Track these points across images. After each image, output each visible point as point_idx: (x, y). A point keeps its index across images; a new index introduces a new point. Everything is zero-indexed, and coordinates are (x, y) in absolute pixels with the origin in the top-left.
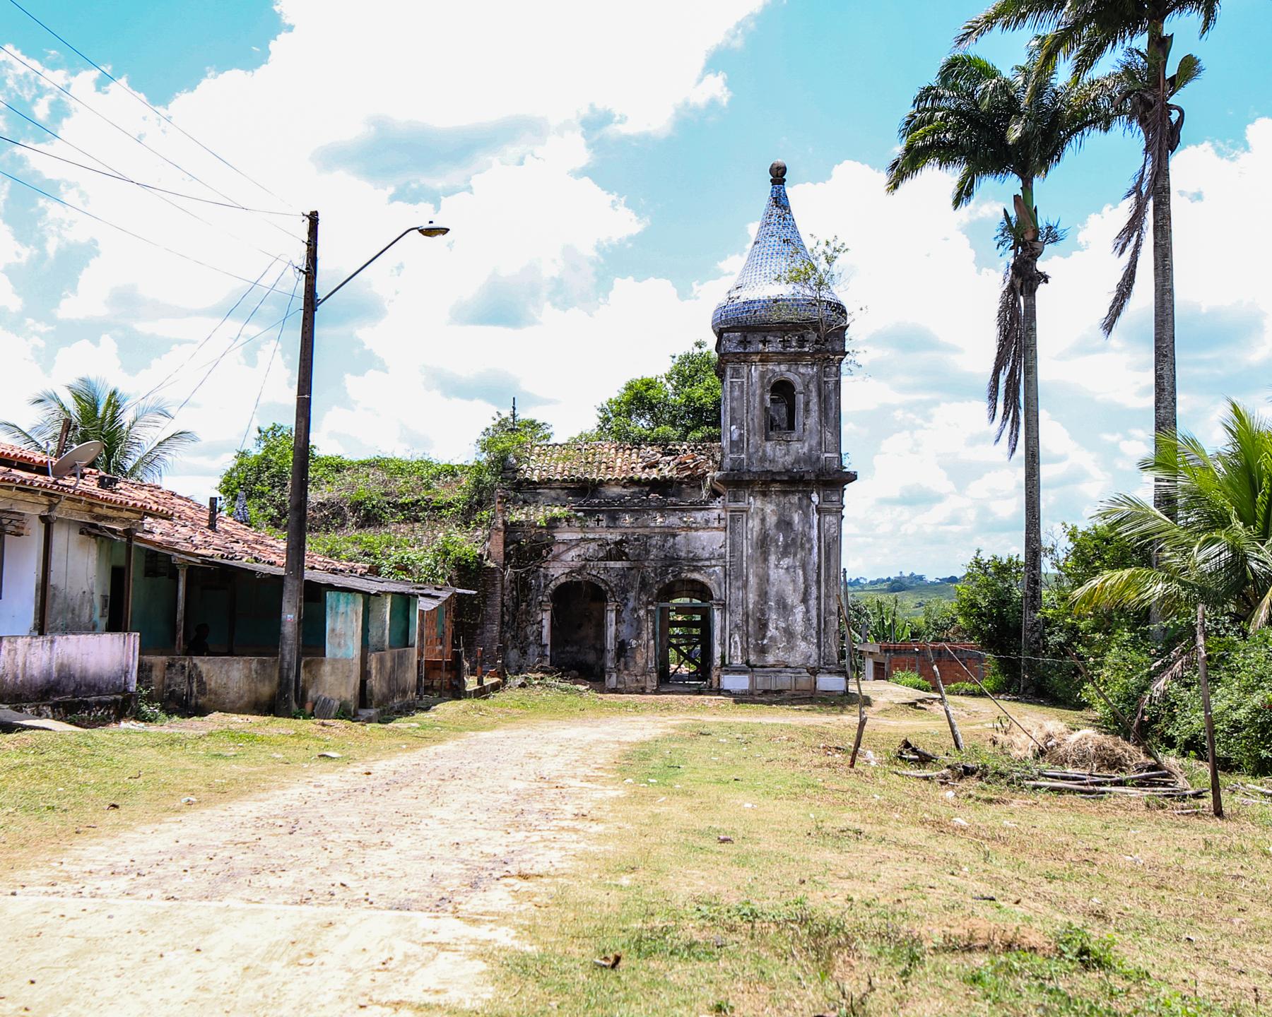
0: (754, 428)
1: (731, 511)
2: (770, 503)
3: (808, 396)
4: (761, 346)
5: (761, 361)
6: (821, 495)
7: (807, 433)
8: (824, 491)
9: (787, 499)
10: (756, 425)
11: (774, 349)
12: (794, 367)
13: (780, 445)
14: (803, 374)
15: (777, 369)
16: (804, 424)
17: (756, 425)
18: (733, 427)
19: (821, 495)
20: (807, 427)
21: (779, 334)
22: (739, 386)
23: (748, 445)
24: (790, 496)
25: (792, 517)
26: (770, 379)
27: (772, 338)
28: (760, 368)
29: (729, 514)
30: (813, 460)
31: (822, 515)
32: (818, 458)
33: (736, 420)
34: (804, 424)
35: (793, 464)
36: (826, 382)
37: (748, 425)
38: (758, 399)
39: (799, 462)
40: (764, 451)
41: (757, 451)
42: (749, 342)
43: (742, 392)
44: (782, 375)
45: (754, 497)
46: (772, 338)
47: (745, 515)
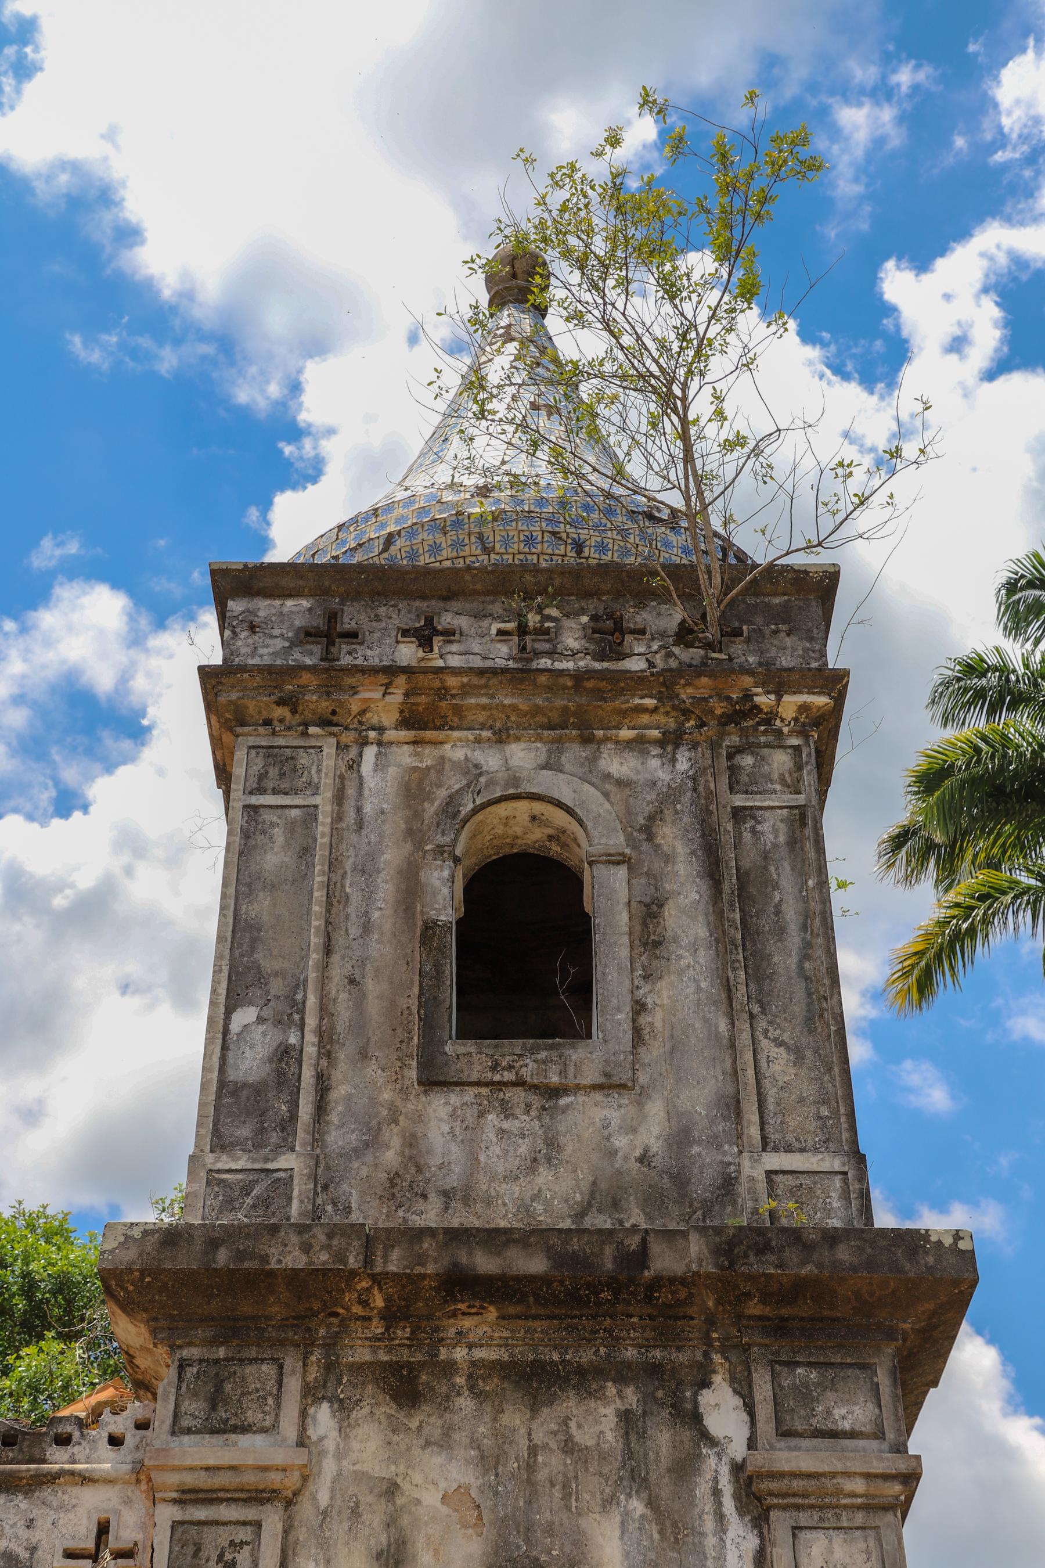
0: (359, 1025)
1: (188, 1497)
2: (444, 1443)
3: (654, 879)
4: (408, 653)
5: (410, 720)
6: (763, 1390)
7: (655, 1050)
8: (777, 1364)
9: (546, 1423)
10: (374, 1008)
11: (477, 662)
12: (574, 753)
13: (506, 1110)
15: (491, 760)
16: (639, 1008)
17: (374, 1008)
18: (244, 1017)
19: (763, 1390)
20: (656, 1019)
21: (497, 608)
22: (291, 827)
23: (321, 1109)
24: (569, 1404)
25: (579, 1541)
26: (452, 801)
27: (462, 622)
28: (404, 756)
29: (167, 1513)
30: (702, 1185)
31: (780, 1523)
32: (728, 1184)
33: (261, 978)
34: (639, 1008)
35: (581, 1215)
36: (739, 814)
37: (324, 1010)
38: (386, 890)
39: (616, 1204)
40: (411, 1141)
41: (372, 1142)
42: (352, 635)
43: (306, 851)
44: (515, 781)
45: (343, 1408)
46: (462, 622)
47: (272, 1520)
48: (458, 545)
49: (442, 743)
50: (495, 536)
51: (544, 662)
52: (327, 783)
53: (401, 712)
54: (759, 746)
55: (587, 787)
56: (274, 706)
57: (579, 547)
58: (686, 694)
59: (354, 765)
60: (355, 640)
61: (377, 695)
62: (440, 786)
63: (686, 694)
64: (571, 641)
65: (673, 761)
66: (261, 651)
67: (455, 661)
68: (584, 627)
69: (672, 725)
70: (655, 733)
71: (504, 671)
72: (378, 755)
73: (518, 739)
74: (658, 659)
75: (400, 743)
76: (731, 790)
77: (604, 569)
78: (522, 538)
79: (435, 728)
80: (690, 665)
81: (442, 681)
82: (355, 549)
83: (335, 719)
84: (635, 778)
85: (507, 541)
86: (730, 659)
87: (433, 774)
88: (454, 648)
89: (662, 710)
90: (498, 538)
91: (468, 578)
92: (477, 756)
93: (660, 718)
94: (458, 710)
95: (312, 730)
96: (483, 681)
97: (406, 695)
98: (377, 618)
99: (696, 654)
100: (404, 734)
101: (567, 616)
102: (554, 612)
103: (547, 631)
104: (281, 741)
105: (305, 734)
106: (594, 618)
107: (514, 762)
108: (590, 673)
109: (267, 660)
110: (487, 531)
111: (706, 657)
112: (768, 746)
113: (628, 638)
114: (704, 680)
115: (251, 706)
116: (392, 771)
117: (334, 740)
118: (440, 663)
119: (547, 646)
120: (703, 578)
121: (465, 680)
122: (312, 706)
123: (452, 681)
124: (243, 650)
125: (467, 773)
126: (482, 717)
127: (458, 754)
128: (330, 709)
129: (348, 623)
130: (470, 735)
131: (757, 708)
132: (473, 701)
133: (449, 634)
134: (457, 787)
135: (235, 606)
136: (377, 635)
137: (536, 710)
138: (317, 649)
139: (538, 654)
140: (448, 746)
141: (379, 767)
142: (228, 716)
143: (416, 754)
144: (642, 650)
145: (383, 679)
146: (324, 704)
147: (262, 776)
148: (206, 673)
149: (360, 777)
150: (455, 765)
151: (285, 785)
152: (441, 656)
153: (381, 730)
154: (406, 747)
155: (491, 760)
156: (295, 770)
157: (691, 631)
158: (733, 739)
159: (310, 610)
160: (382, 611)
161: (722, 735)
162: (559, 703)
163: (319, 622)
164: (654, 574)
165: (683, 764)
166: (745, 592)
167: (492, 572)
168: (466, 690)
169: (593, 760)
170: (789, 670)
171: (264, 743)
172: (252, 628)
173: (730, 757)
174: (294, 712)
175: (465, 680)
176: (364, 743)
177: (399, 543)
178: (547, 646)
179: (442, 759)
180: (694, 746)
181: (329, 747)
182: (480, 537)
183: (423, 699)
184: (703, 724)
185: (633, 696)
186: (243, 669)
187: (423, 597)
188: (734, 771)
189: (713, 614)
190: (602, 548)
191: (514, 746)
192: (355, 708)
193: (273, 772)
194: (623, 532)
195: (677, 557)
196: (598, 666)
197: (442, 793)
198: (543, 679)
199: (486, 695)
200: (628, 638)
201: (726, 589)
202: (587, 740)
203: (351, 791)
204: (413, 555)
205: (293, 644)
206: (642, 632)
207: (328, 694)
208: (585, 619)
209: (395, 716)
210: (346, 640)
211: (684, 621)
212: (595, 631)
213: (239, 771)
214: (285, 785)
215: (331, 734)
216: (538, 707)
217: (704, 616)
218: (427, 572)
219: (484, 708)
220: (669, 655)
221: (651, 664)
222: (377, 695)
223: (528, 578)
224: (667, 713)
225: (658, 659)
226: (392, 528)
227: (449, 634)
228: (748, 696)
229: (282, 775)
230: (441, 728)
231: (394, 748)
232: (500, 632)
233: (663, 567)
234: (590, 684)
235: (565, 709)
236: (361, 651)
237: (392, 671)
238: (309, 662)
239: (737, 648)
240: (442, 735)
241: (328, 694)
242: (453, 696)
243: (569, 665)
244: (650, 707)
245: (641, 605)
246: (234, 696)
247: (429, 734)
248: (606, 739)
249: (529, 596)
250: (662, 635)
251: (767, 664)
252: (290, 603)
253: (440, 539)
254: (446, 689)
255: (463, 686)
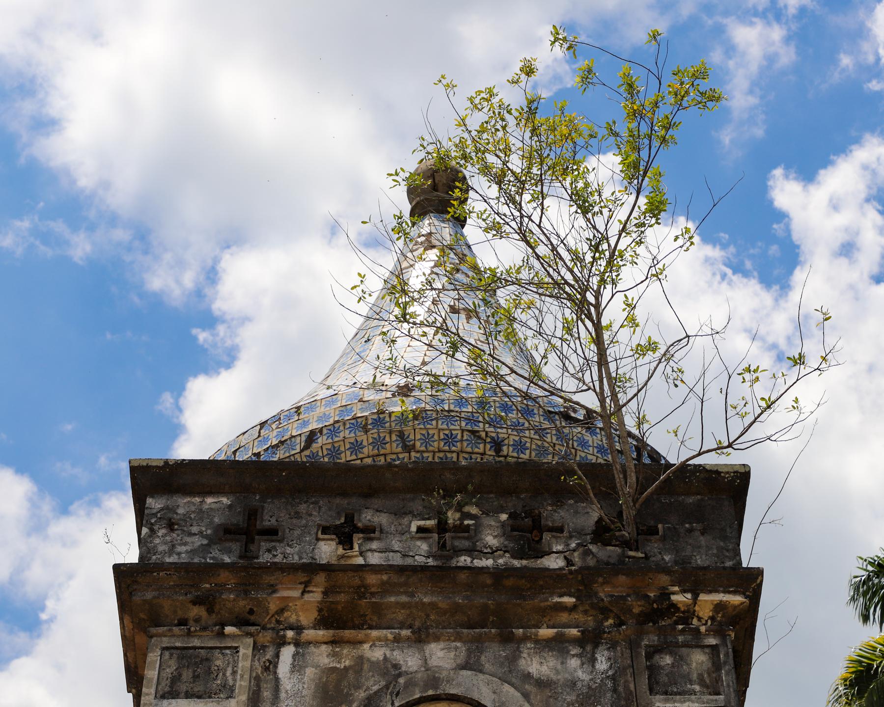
11: (397, 560)
12: (492, 655)
14: (542, 684)
15: (410, 660)
21: (417, 506)
27: (383, 519)
28: (322, 656)
42: (272, 533)
44: (433, 681)
46: (383, 519)
48: (379, 442)
49: (361, 642)
50: (415, 433)
51: (464, 560)
52: (242, 684)
53: (320, 610)
54: (677, 645)
55: (507, 687)
56: (190, 606)
57: (497, 445)
58: (604, 592)
59: (271, 666)
60: (275, 537)
61: (296, 593)
62: (358, 687)
63: (604, 592)
64: (491, 540)
65: (593, 661)
66: (179, 549)
67: (375, 559)
68: (503, 525)
69: (590, 622)
70: (574, 632)
71: (424, 568)
72: (294, 656)
73: (437, 639)
74: (576, 557)
75: (317, 643)
76: (651, 691)
77: (523, 468)
78: (442, 437)
79: (354, 627)
80: (608, 563)
81: (362, 579)
82: (276, 446)
83: (252, 618)
84: (554, 678)
85: (427, 439)
86: (647, 558)
87: (351, 676)
88: (375, 545)
89: (581, 608)
90: (418, 436)
91: (388, 475)
92: (397, 656)
93: (578, 617)
94: (377, 609)
95: (229, 629)
96: (402, 580)
97: (325, 593)
98: (298, 515)
99: (613, 551)
100: (321, 634)
101: (486, 513)
102: (474, 510)
103: (467, 529)
104: (196, 642)
105: (221, 634)
106: (512, 516)
107: (434, 662)
108: (509, 571)
109: (184, 558)
110: (408, 430)
111: (624, 555)
112: (686, 645)
113: (547, 536)
114: (622, 578)
115: (167, 605)
116: (310, 672)
117: (250, 641)
118: (360, 561)
119: (466, 544)
120: (618, 477)
121: (385, 577)
122: (229, 605)
123: (372, 579)
124: (161, 548)
125: (384, 674)
126: (401, 615)
127: (377, 654)
128: (248, 607)
129: (268, 521)
130: (388, 634)
131: (674, 606)
132: (393, 599)
133: (369, 532)
134: (375, 688)
135: (154, 504)
136: (297, 532)
137: (456, 609)
138: (236, 547)
139: (458, 552)
140: (366, 646)
141: (297, 667)
142: (142, 616)
143: (334, 655)
144: (560, 548)
145: (302, 577)
146: (242, 603)
147: (175, 679)
148: (121, 572)
149: (277, 680)
150: (374, 665)
151: (199, 688)
152: (361, 554)
153: (299, 629)
154: (324, 647)
155: (410, 660)
156: (209, 672)
157: (607, 529)
158: (651, 639)
159: (230, 507)
160: (303, 508)
161: (640, 634)
162: (479, 601)
163: (238, 519)
164: (571, 472)
165: (602, 664)
166: (660, 490)
167: (412, 470)
168: (386, 588)
169: (514, 658)
170: (705, 569)
171: (178, 644)
172: (171, 526)
173: (649, 657)
174: (210, 611)
175: (385, 577)
176: (282, 642)
177: (321, 440)
178: (466, 544)
179: (361, 659)
180: (613, 646)
181: (245, 650)
182: (401, 435)
183: (342, 598)
184: (622, 623)
185: (552, 594)
186: (161, 566)
187: (344, 494)
188: (653, 670)
189: (629, 513)
190: (520, 446)
191: (433, 646)
192: (273, 607)
193: (187, 675)
194: (541, 432)
195: (592, 456)
196: (517, 563)
197: (362, 694)
198: (463, 576)
199: (406, 593)
200: (547, 536)
201: (641, 487)
202: (507, 639)
203: (266, 694)
204: (334, 451)
205: (213, 541)
206: (561, 530)
207: (246, 592)
208: (504, 517)
209: (314, 615)
210: (265, 537)
211: (600, 520)
212: (513, 530)
213: (151, 674)
214: (199, 688)
215: (250, 634)
216: (458, 604)
217: (620, 514)
218: (348, 468)
219: (403, 606)
220: (588, 553)
221: (569, 563)
222: (296, 593)
223: (448, 475)
224: (585, 612)
225: (576, 557)
226: (314, 426)
227: (369, 532)
228: (665, 595)
229: (196, 677)
230: (359, 627)
231: (312, 649)
232: (420, 530)
233: (580, 465)
234: (509, 582)
235: (485, 607)
236: (280, 548)
237: (312, 569)
238: (227, 560)
239: (654, 546)
240: (360, 634)
241: (246, 592)
242: (373, 594)
243: (489, 563)
244: (569, 605)
245: (559, 503)
246: (149, 595)
247: (348, 633)
248: (525, 639)
249: (449, 494)
250: (579, 533)
251: (682, 562)
252: (209, 500)
253: (362, 437)
254: (366, 587)
255: (383, 583)
